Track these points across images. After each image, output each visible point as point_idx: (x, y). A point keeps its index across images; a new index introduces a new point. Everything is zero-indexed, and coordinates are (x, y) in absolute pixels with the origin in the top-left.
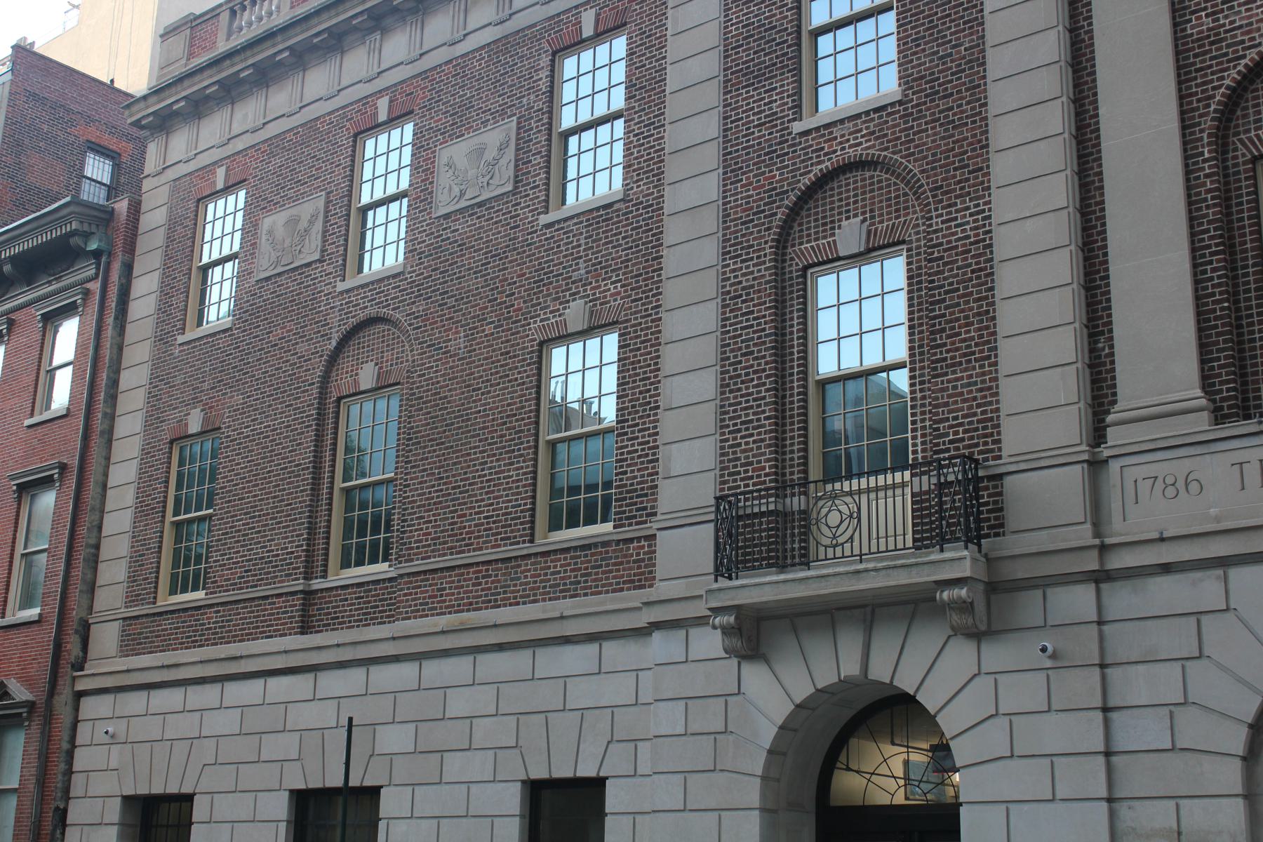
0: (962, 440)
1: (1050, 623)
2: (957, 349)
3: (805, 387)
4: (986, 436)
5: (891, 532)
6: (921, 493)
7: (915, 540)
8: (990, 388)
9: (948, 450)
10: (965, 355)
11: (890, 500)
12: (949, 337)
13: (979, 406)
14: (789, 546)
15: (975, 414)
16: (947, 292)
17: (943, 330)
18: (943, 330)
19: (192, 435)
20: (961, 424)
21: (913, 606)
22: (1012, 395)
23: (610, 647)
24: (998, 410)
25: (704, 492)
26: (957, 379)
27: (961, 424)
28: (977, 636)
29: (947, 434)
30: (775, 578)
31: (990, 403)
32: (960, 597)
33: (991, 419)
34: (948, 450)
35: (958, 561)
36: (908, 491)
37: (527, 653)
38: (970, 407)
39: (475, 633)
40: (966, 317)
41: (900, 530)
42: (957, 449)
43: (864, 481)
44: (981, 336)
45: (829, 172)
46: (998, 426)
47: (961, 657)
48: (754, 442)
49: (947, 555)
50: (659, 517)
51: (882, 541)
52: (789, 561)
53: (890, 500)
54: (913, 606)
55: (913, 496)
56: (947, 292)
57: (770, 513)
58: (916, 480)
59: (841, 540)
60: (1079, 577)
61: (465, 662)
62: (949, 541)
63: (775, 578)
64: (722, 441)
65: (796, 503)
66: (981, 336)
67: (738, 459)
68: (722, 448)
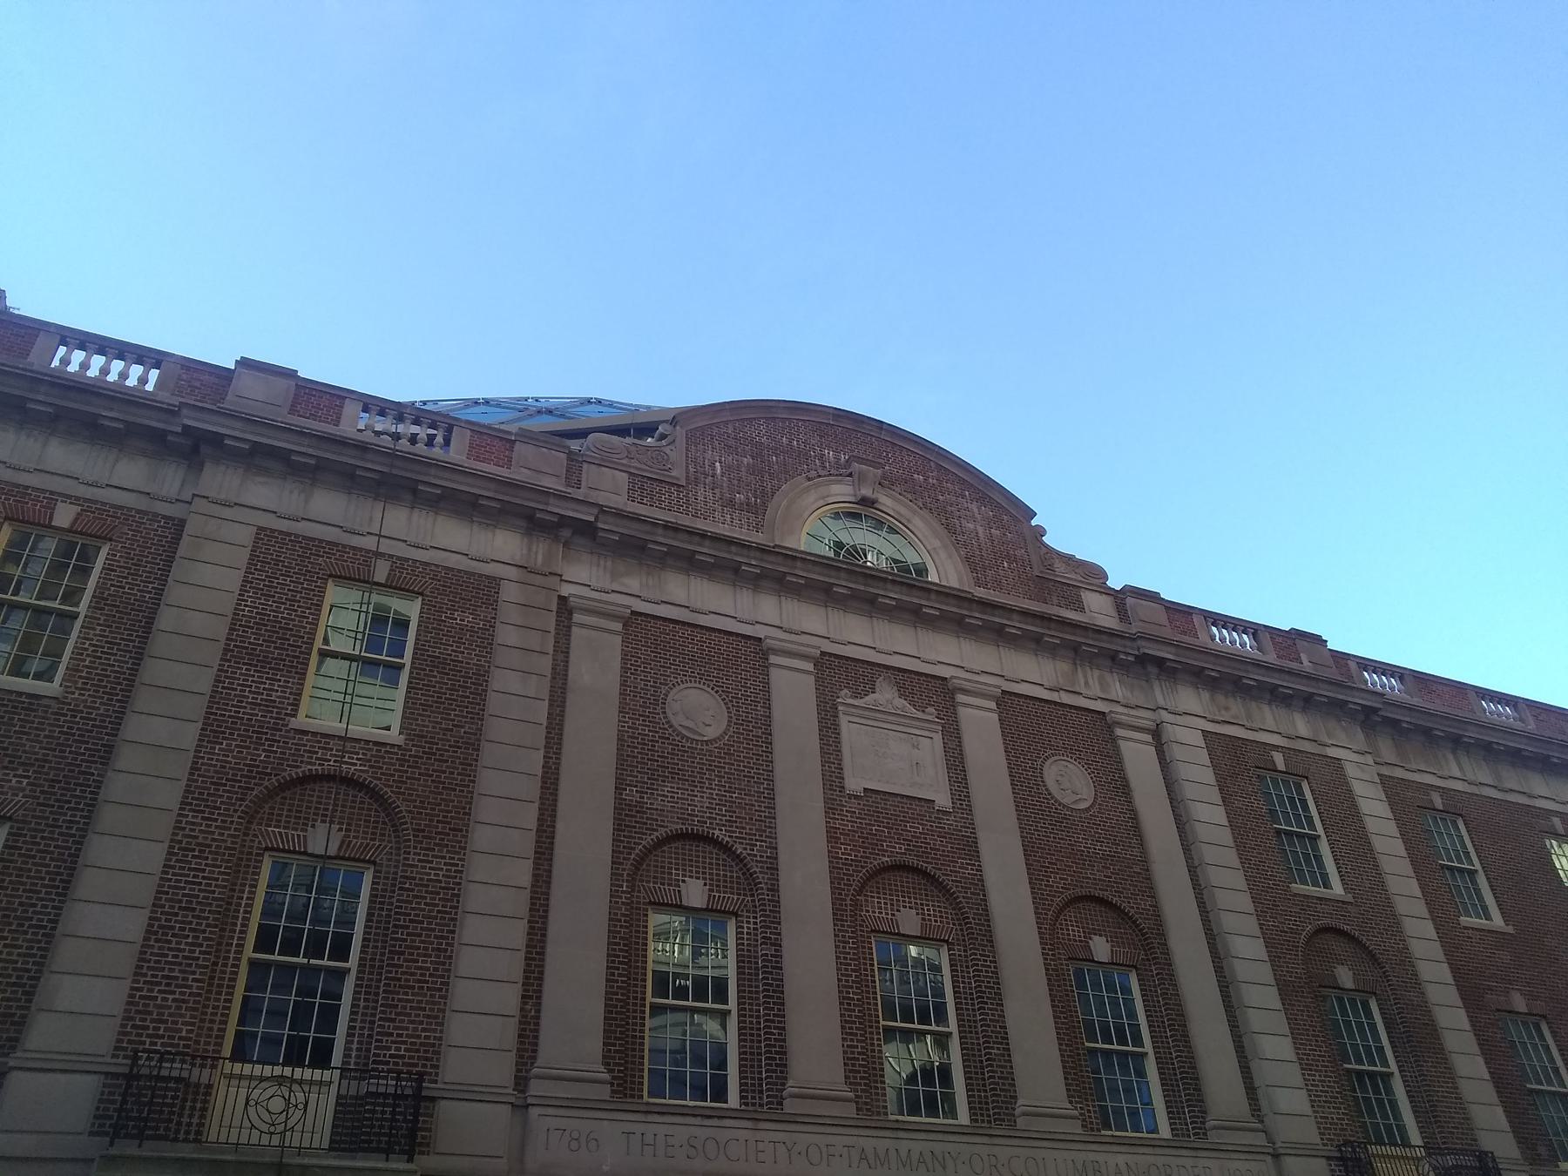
0: (403, 1057)
2: (413, 974)
3: (239, 959)
4: (427, 1059)
5: (226, 1122)
6: (345, 1097)
7: (332, 1141)
8: (436, 1017)
9: (387, 1063)
10: (419, 981)
11: (233, 1090)
12: (406, 960)
13: (424, 1030)
14: (185, 1120)
15: (419, 1037)
16: (411, 921)
17: (403, 953)
18: (403, 953)
20: (404, 1043)
22: (458, 1029)
24: (440, 1039)
25: (99, 1039)
26: (408, 1001)
27: (404, 1043)
29: (389, 1049)
31: (435, 1031)
33: (433, 1045)
34: (387, 1063)
36: (334, 1088)
38: (415, 1029)
40: (426, 949)
42: (396, 1064)
44: (436, 969)
46: (439, 1053)
48: (174, 1000)
50: (19, 1054)
51: (224, 1131)
52: (181, 1136)
55: (339, 1096)
56: (411, 921)
57: (178, 1080)
58: (345, 1083)
64: (132, 989)
65: (201, 1075)
66: (436, 969)
67: (150, 1013)
68: (131, 996)
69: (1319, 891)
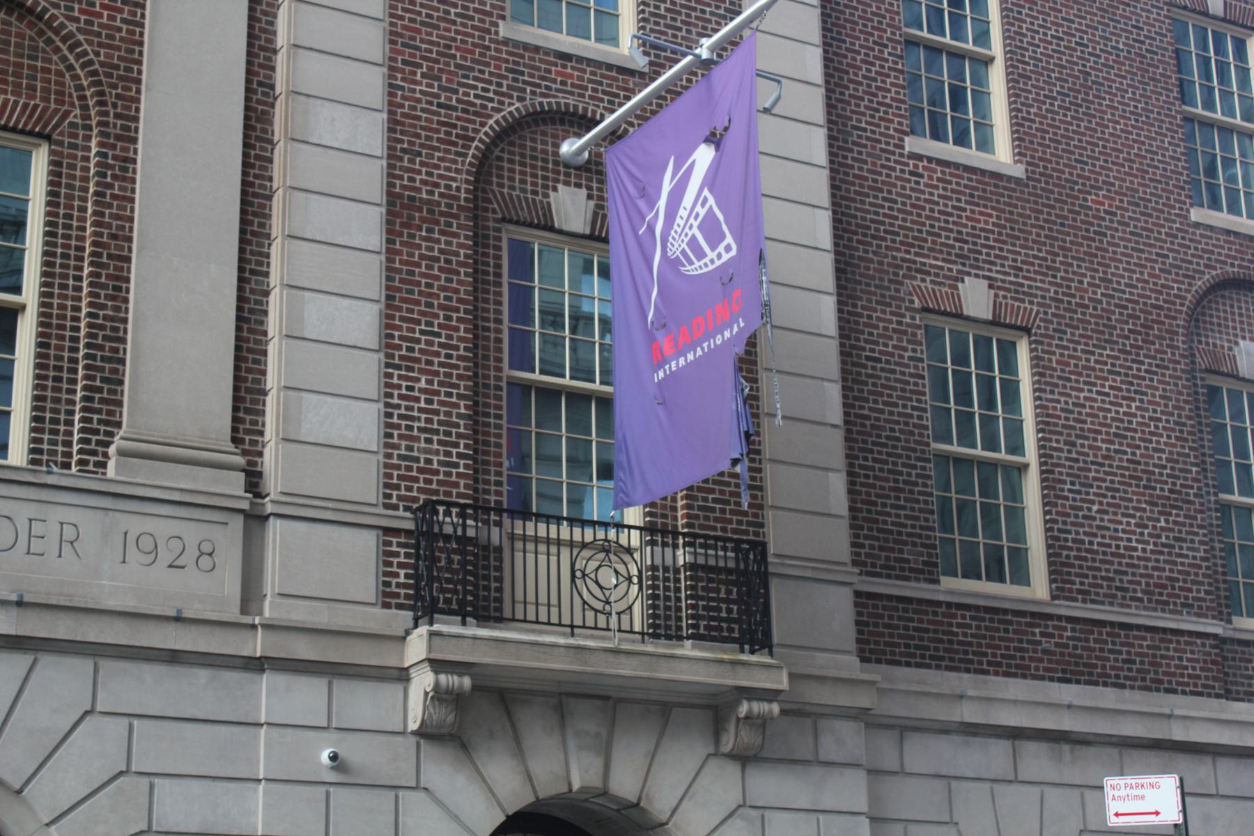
1: (99, 708)
19: (968, 318)
21: (663, 710)
23: (346, 690)
28: (745, 759)
30: (457, 630)
32: (461, 686)
35: (694, 663)
37: (86, 665)
39: (218, 631)
41: (554, 601)
43: (530, 526)
45: (575, 114)
47: (723, 785)
49: (754, 658)
53: (553, 559)
54: (663, 710)
59: (617, 607)
60: (238, 661)
61: (1001, 748)
62: (442, 612)
63: (457, 630)
69: (590, 47)
